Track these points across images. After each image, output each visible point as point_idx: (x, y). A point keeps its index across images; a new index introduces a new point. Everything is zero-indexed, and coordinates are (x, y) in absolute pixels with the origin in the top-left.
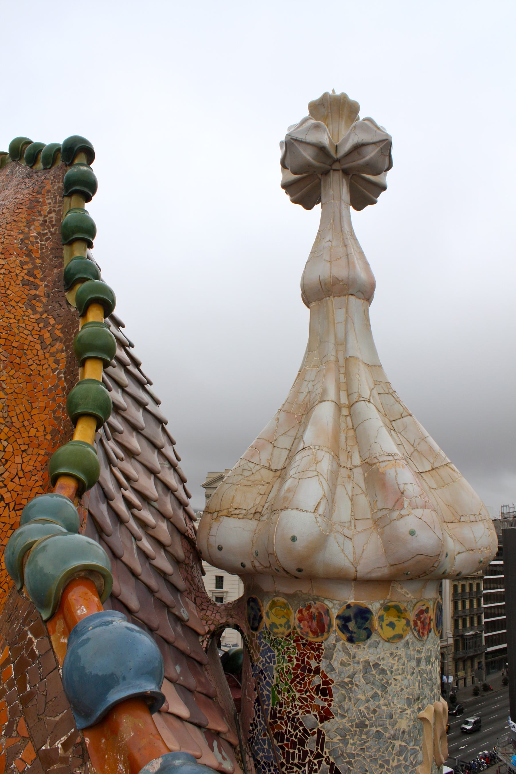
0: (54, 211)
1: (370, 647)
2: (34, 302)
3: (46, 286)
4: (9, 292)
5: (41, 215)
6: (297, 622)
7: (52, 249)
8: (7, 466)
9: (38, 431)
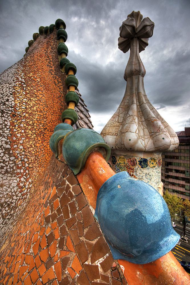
0: (55, 44)
1: (147, 169)
4: (43, 67)
5: (51, 46)
6: (127, 162)
7: (55, 56)
8: (47, 119)
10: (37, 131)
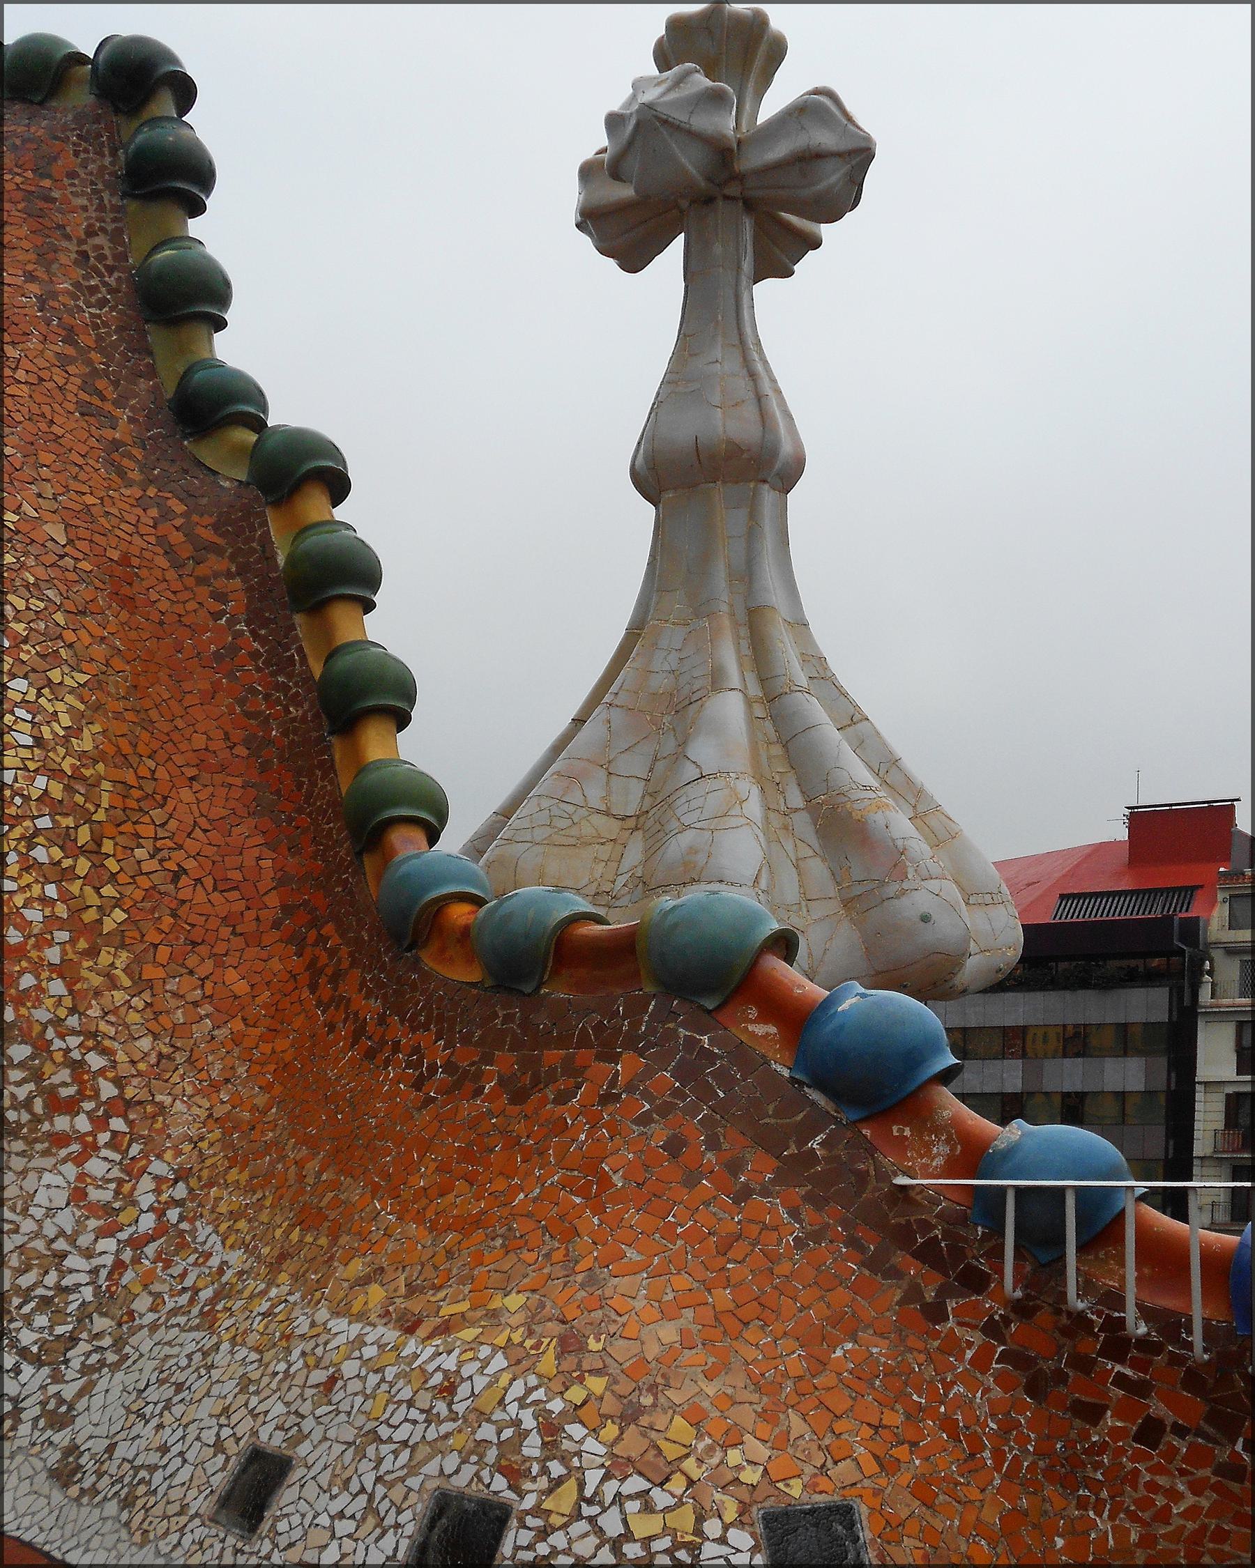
2: (115, 455)
3: (131, 420)
8: (169, 807)
9: (209, 738)
10: (128, 890)
